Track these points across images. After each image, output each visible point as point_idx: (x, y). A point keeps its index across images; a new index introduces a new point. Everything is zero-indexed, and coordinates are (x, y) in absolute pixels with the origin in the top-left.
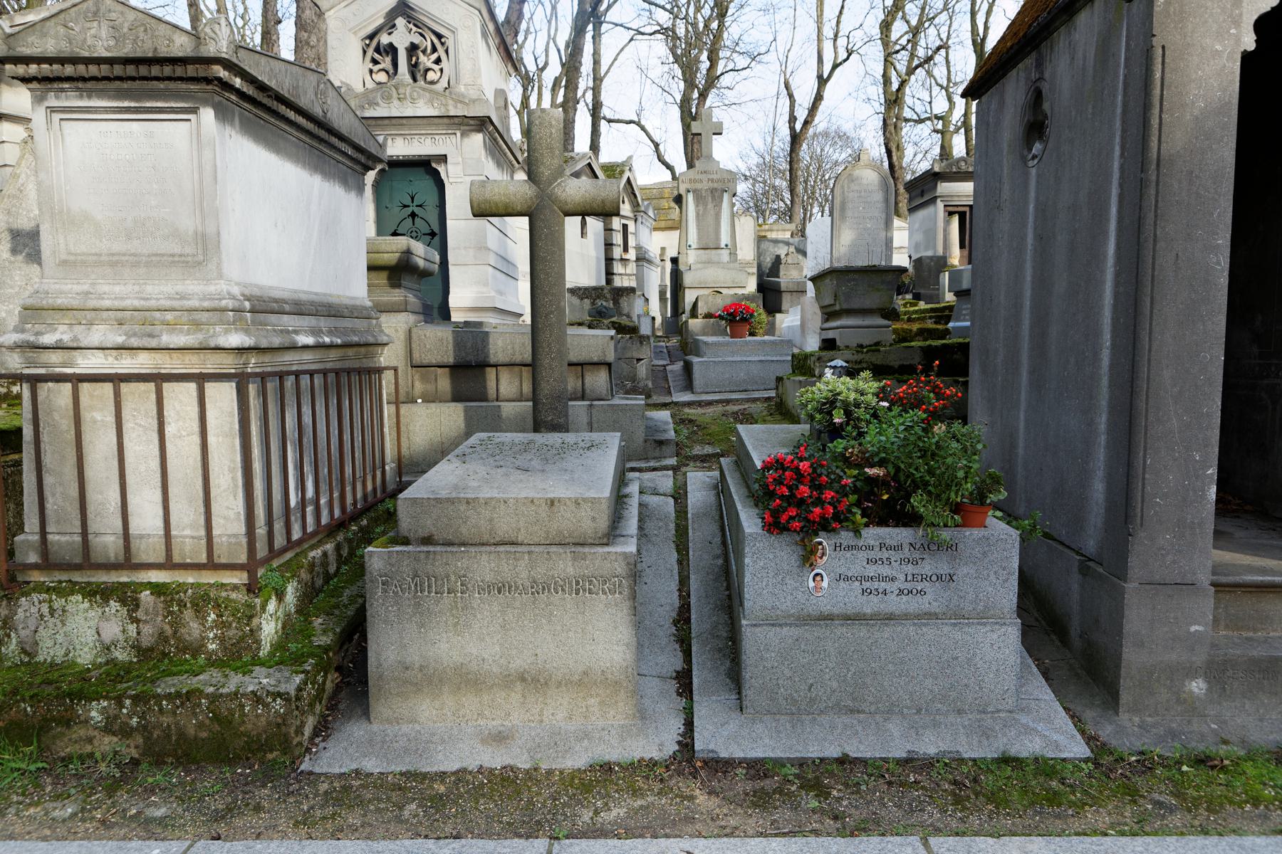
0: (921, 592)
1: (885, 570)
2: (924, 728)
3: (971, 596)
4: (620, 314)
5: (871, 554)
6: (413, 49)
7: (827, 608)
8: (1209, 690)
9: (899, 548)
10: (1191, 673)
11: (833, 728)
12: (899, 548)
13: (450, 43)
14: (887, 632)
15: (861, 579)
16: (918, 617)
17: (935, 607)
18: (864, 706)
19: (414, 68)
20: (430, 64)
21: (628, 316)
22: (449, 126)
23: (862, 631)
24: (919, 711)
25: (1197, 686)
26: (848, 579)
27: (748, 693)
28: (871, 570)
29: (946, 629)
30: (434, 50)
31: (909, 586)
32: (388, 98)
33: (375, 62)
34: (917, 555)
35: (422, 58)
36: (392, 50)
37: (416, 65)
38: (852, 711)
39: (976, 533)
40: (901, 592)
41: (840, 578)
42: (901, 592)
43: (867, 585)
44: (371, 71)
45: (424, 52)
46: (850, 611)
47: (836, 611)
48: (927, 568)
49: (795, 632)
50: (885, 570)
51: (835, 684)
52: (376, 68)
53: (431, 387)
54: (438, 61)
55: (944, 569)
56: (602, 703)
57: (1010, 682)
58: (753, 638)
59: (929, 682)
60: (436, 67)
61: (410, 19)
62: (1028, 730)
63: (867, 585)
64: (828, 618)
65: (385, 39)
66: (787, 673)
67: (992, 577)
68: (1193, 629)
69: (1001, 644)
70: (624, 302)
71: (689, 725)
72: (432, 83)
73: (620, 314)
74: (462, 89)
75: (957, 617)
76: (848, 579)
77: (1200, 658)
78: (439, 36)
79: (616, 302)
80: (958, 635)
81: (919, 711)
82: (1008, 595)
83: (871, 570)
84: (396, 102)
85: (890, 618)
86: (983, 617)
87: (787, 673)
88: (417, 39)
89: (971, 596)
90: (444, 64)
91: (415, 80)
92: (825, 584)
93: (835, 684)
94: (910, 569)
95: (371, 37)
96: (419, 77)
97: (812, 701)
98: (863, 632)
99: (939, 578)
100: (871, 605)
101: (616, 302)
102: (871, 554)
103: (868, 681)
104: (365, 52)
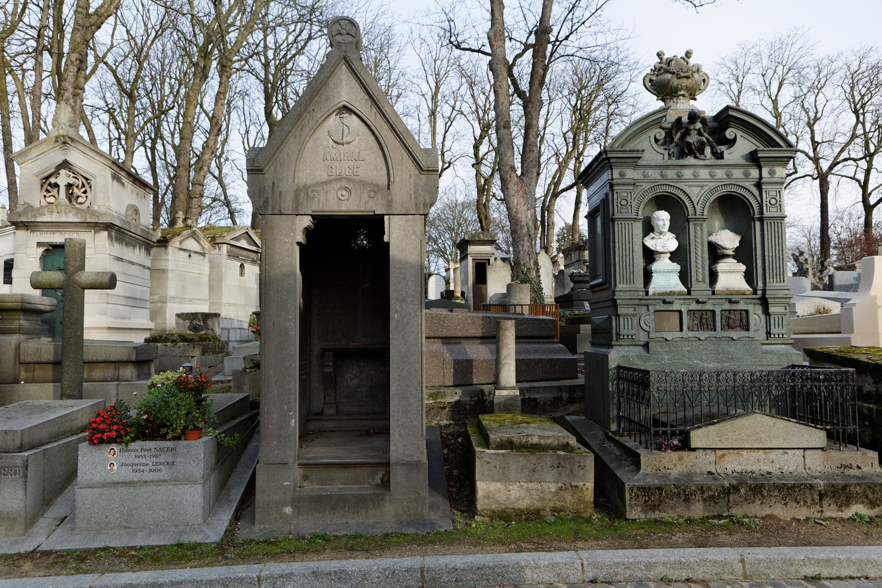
0: (160, 470)
1: (143, 461)
3: (182, 472)
4: (207, 329)
5: (137, 453)
6: (69, 186)
7: (116, 479)
8: (293, 511)
9: (149, 450)
10: (285, 504)
12: (150, 450)
13: (92, 183)
14: (143, 489)
15: (132, 465)
16: (158, 481)
17: (166, 477)
18: (132, 525)
19: (70, 197)
20: (80, 194)
21: (212, 330)
22: (87, 227)
24: (157, 526)
25: (288, 510)
26: (126, 465)
28: (137, 461)
29: (169, 487)
30: (83, 186)
31: (154, 468)
32: (52, 212)
33: (48, 191)
35: (76, 190)
36: (56, 185)
37: (72, 194)
38: (126, 528)
40: (150, 470)
41: (122, 465)
42: (150, 470)
43: (135, 468)
44: (45, 196)
45: (77, 187)
46: (127, 480)
47: (120, 480)
48: (162, 459)
49: (99, 490)
50: (143, 461)
51: (118, 515)
52: (48, 195)
53: (30, 375)
54: (85, 192)
55: (170, 459)
56: (7, 529)
59: (162, 513)
60: (84, 195)
61: (70, 170)
63: (135, 468)
64: (117, 483)
65: (53, 180)
66: (96, 511)
67: (192, 462)
68: (286, 483)
70: (210, 322)
72: (80, 203)
73: (207, 329)
74: (96, 207)
75: (175, 481)
76: (126, 465)
77: (288, 497)
78: (87, 179)
79: (205, 322)
80: (175, 490)
81: (157, 526)
83: (137, 461)
84: (55, 214)
85: (146, 482)
86: (189, 481)
87: (96, 511)
88: (72, 181)
89: (182, 472)
90: (88, 194)
91: (70, 201)
92: (115, 468)
93: (118, 515)
94: (154, 460)
95: (47, 178)
96: (73, 200)
97: (108, 524)
98: (131, 489)
100: (136, 477)
101: (205, 322)
102: (137, 453)
103: (134, 513)
104: (42, 186)
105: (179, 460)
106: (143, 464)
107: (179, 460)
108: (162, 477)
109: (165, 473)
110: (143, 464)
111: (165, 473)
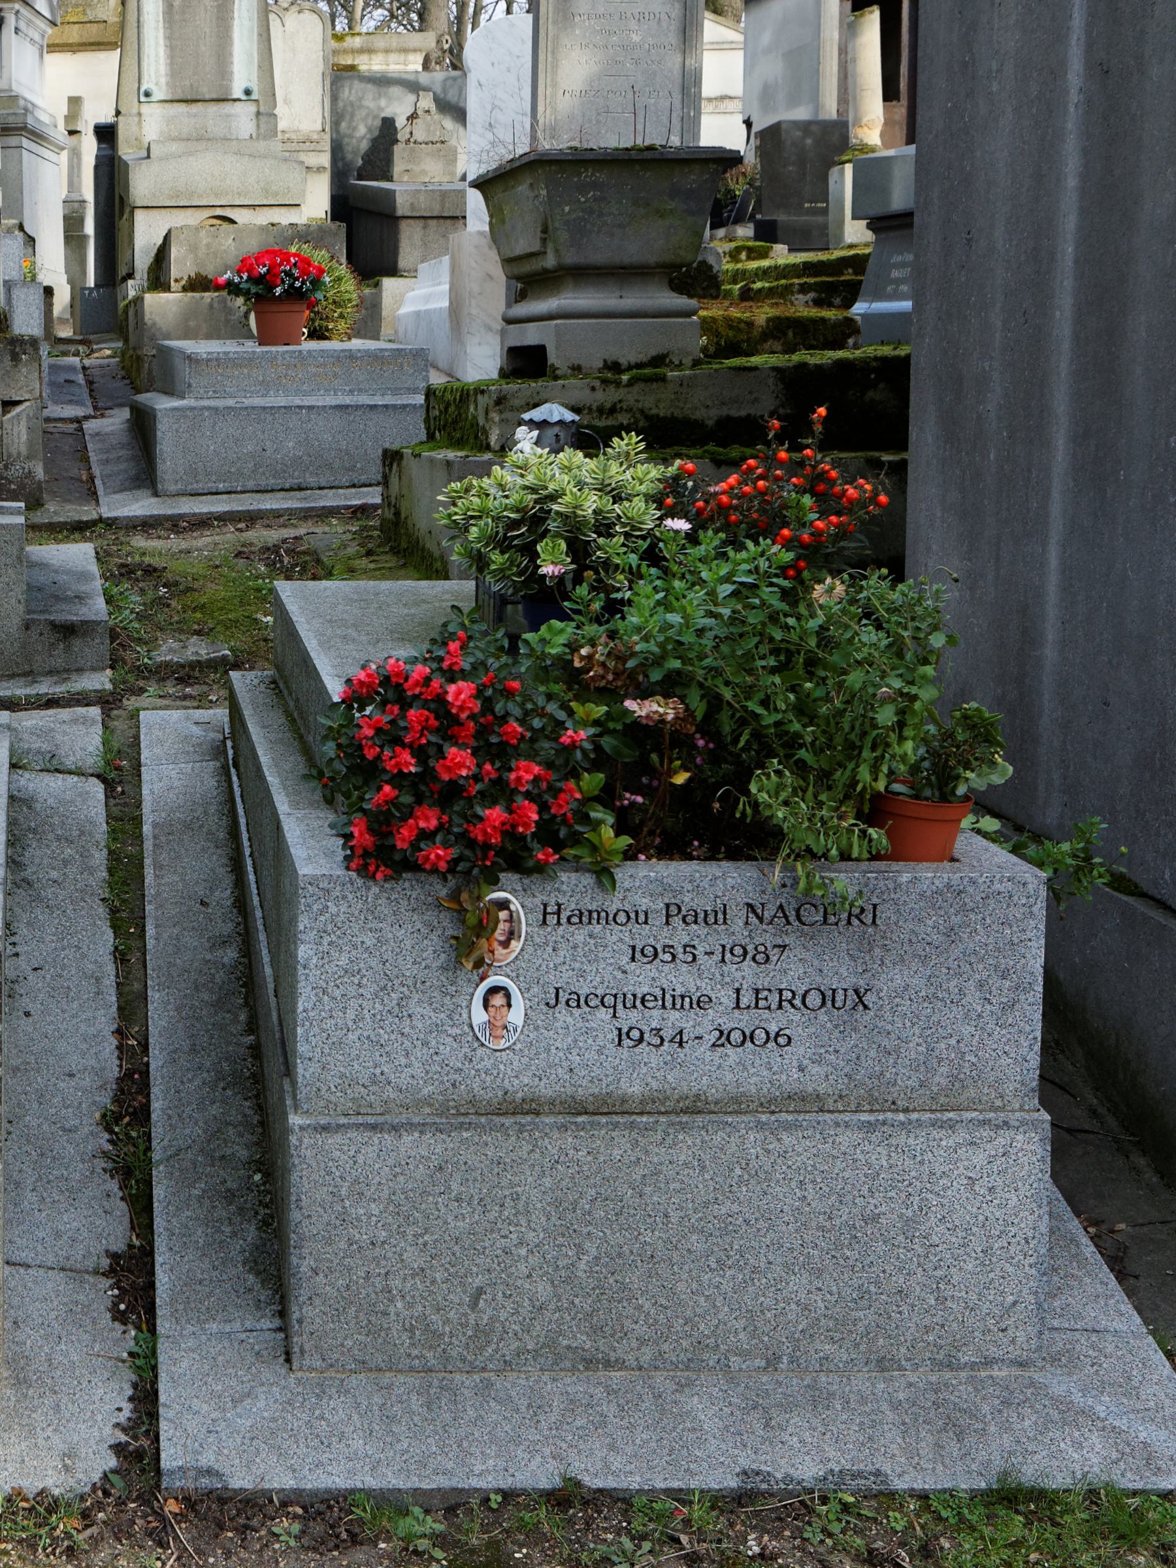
1: (680, 979)
2: (788, 1406)
3: (914, 1049)
5: (643, 935)
7: (520, 1078)
9: (717, 917)
11: (537, 1408)
12: (717, 917)
14: (686, 1147)
15: (615, 1002)
16: (771, 1105)
17: (816, 1080)
18: (622, 1350)
23: (616, 1145)
24: (772, 1363)
26: (578, 1001)
27: (308, 1313)
28: (643, 979)
29: (846, 1139)
31: (745, 1021)
34: (766, 937)
39: (920, 877)
42: (723, 1037)
43: (630, 1018)
46: (586, 1089)
47: (545, 1090)
48: (794, 971)
49: (433, 1146)
50: (680, 979)
51: (543, 1290)
55: (841, 974)
57: (1019, 1279)
58: (325, 1165)
59: (798, 1284)
62: (1071, 1415)
63: (630, 1018)
64: (526, 1108)
67: (973, 998)
69: (997, 1177)
71: (146, 1399)
75: (876, 1104)
76: (578, 1001)
80: (879, 1156)
81: (772, 1363)
82: (1013, 1046)
83: (643, 979)
85: (694, 1108)
86: (947, 1104)
89: (914, 1049)
92: (516, 1016)
93: (543, 1290)
94: (747, 974)
97: (482, 1334)
99: (828, 998)
100: (641, 1073)
102: (643, 935)
103: (634, 1279)
105: (892, 979)
106: (681, 1001)
107: (892, 979)
108: (791, 1079)
109: (806, 1056)
110: (681, 1001)
111: (806, 1056)
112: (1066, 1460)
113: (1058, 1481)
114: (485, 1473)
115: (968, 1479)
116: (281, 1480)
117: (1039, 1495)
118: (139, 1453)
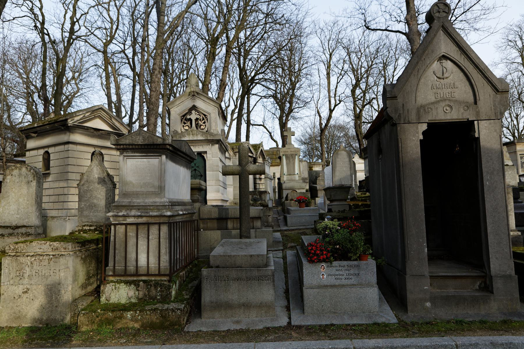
1: (341, 273)
2: (354, 316)
3: (364, 280)
4: (262, 200)
6: (197, 119)
7: (326, 284)
8: (432, 305)
9: (344, 266)
11: (329, 317)
12: (344, 266)
13: (208, 117)
14: (342, 290)
17: (355, 283)
19: (197, 125)
20: (202, 124)
21: (265, 201)
22: (208, 142)
23: (336, 290)
24: (352, 312)
25: (428, 304)
26: (331, 275)
27: (306, 308)
28: (337, 273)
29: (358, 289)
30: (203, 119)
31: (347, 277)
32: (189, 134)
33: (185, 123)
34: (349, 268)
35: (200, 122)
36: (190, 120)
37: (198, 124)
39: (363, 262)
40: (345, 279)
41: (329, 275)
44: (183, 126)
45: (200, 120)
46: (332, 284)
47: (328, 284)
48: (352, 272)
49: (317, 290)
50: (341, 273)
51: (329, 305)
52: (185, 125)
53: (205, 226)
54: (204, 123)
55: (357, 272)
56: (266, 312)
57: (377, 303)
58: (307, 292)
59: (354, 304)
60: (204, 125)
61: (196, 110)
62: (382, 317)
65: (188, 117)
68: (425, 288)
69: (373, 293)
70: (263, 196)
71: (290, 318)
72: (203, 129)
73: (262, 200)
74: (212, 131)
75: (361, 285)
76: (331, 275)
78: (205, 115)
79: (260, 196)
81: (352, 312)
82: (374, 279)
83: (337, 273)
84: (191, 136)
86: (369, 285)
88: (198, 117)
89: (364, 280)
90: (206, 124)
91: (197, 128)
92: (325, 277)
93: (329, 305)
94: (347, 272)
95: (184, 116)
96: (198, 127)
97: (323, 310)
98: (336, 290)
99: (355, 274)
100: (338, 282)
101: (260, 196)
103: (338, 304)
104: (182, 121)
105: (362, 272)
106: (341, 275)
107: (362, 272)
108: (352, 283)
109: (354, 280)
110: (341, 275)
111: (354, 280)
112: (381, 320)
113: (380, 322)
114: (324, 323)
115: (371, 322)
116: (303, 324)
117: (378, 324)
118: (289, 323)
